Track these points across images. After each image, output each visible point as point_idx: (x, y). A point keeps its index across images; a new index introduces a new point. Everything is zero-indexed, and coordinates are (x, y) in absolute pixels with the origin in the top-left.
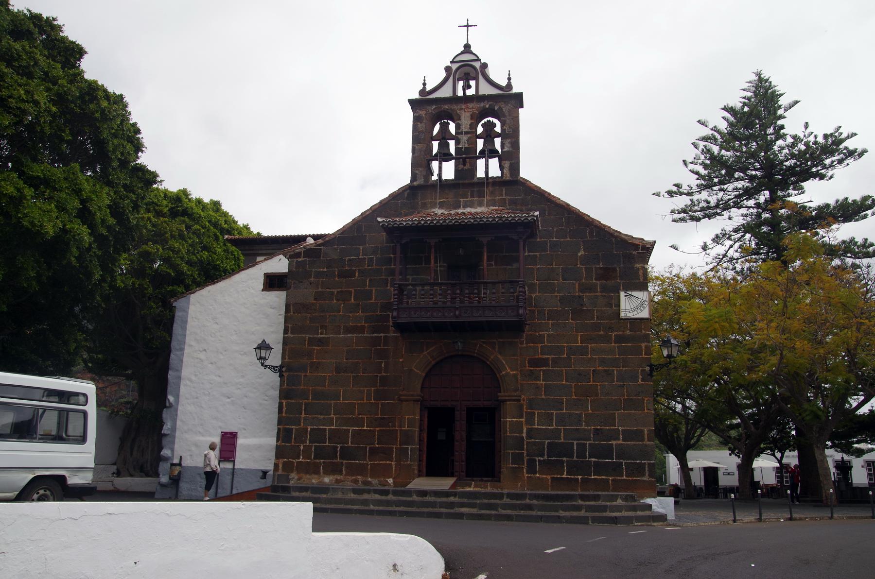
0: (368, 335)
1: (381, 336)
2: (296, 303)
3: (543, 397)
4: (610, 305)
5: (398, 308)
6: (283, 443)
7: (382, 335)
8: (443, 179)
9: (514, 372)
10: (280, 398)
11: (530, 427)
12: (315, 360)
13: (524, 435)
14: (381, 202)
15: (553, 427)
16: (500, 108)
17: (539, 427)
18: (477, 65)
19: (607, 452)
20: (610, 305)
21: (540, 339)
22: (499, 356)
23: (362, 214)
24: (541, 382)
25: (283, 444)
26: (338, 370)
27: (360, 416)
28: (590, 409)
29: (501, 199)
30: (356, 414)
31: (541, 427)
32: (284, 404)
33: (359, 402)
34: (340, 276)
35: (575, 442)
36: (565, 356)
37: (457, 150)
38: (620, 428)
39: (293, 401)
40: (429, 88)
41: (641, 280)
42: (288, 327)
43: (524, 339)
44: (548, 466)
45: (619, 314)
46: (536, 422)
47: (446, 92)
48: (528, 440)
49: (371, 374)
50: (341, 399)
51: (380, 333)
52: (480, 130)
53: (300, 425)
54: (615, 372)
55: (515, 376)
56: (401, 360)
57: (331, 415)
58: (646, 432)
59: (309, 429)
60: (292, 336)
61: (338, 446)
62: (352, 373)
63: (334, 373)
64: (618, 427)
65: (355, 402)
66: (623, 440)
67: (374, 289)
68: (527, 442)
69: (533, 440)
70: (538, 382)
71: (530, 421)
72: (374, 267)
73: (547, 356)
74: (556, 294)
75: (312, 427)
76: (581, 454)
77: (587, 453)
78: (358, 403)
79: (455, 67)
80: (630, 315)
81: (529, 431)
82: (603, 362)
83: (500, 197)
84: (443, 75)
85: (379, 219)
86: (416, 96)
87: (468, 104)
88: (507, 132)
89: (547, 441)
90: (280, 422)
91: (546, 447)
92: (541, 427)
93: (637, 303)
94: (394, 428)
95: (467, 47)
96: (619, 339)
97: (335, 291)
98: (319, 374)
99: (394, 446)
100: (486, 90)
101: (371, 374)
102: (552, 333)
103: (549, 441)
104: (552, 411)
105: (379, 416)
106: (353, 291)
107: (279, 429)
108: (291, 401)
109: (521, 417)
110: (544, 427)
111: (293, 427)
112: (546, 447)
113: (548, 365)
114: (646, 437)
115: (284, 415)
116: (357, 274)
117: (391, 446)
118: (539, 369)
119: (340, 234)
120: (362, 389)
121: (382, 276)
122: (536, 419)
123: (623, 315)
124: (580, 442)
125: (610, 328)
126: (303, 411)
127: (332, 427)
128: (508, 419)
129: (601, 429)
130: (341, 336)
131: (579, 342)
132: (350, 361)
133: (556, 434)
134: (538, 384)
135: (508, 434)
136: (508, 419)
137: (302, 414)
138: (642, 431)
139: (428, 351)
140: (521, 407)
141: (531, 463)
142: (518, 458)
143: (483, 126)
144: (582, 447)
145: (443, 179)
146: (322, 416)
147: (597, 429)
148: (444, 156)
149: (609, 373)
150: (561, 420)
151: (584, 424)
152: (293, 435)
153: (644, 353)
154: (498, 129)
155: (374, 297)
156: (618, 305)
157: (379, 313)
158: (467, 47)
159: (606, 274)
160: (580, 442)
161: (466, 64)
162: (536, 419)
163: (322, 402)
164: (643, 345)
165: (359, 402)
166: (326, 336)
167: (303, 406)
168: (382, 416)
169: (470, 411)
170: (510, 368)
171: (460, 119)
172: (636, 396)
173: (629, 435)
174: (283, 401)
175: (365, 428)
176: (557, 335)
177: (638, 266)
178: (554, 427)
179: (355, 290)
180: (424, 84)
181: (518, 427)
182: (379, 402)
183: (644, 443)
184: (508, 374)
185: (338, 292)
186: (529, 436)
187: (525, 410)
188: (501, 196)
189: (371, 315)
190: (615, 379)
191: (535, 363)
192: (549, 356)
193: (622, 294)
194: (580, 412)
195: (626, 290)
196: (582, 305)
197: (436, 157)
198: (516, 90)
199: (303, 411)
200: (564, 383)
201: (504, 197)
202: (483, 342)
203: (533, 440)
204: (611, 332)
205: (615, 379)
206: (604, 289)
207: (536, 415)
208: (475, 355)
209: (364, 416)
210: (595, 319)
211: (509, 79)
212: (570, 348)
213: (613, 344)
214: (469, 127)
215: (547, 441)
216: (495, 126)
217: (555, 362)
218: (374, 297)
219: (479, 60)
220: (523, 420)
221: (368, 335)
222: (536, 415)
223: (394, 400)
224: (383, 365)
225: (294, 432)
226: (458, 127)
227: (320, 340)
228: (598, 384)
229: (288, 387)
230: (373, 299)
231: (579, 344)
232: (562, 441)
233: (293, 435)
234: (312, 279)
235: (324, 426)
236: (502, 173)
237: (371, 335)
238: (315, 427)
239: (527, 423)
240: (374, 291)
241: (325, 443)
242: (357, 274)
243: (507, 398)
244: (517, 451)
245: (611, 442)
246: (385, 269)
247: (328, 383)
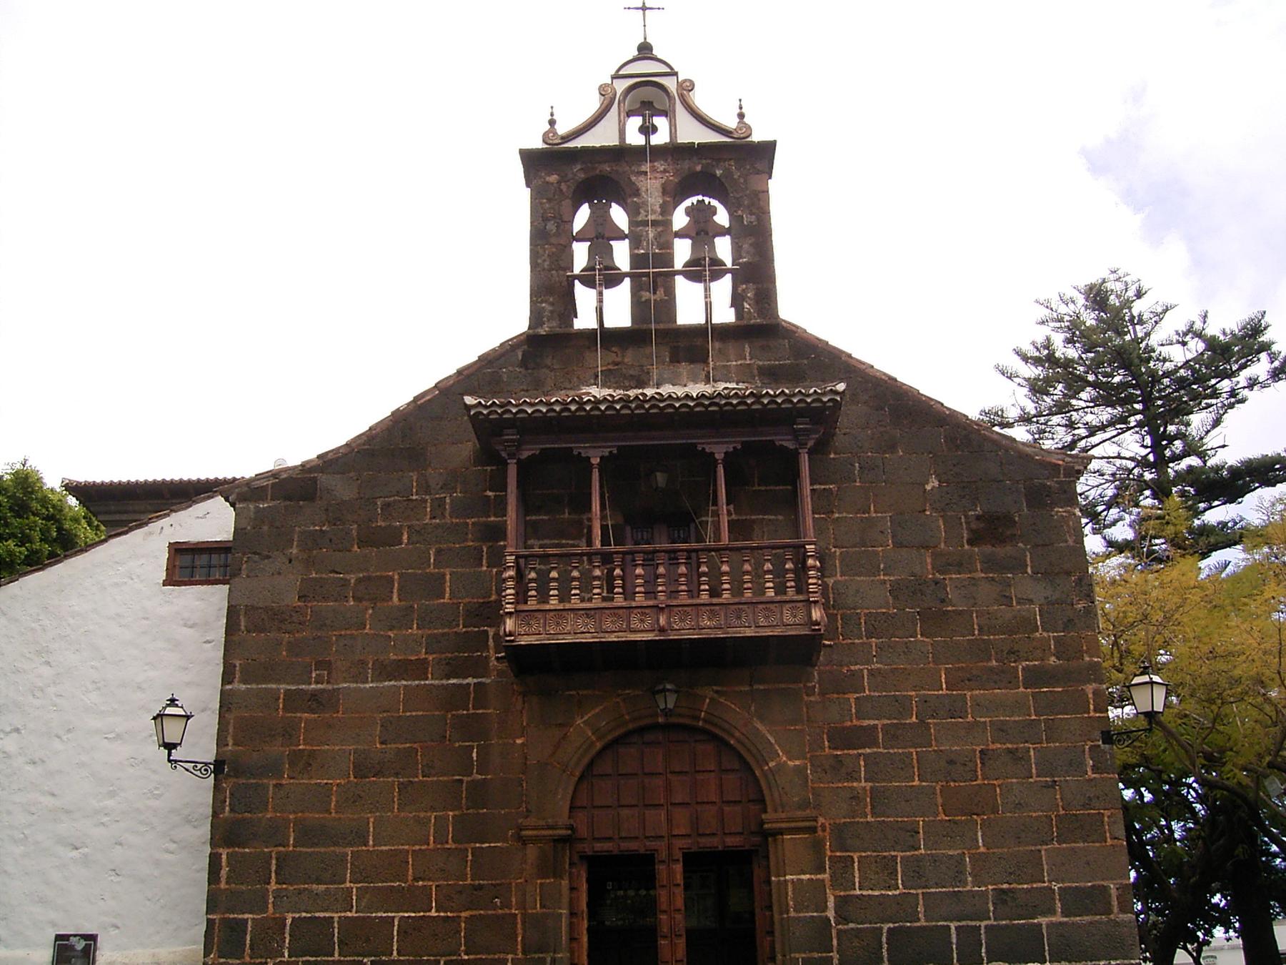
0: (436, 682)
1: (469, 684)
2: (254, 608)
3: (869, 819)
5: (516, 611)
6: (219, 957)
7: (470, 680)
8: (688, 218)
9: (797, 763)
10: (213, 843)
11: (842, 894)
12: (301, 747)
13: (831, 914)
14: (459, 372)
15: (897, 892)
16: (728, 174)
17: (865, 893)
18: (670, 83)
21: (854, 682)
22: (759, 726)
23: (416, 399)
24: (863, 784)
25: (222, 960)
26: (361, 770)
27: (421, 883)
28: (981, 844)
29: (741, 364)
30: (410, 878)
31: (870, 892)
32: (224, 857)
33: (417, 847)
34: (362, 543)
35: (953, 925)
36: (914, 719)
37: (636, 260)
38: (1056, 887)
39: (247, 850)
40: (562, 129)
41: (1071, 542)
42: (235, 666)
43: (815, 682)
46: (857, 880)
47: (602, 137)
48: (840, 927)
49: (445, 778)
50: (371, 843)
51: (466, 678)
52: (680, 219)
53: (265, 909)
54: (1032, 753)
55: (800, 771)
56: (519, 741)
57: (344, 882)
58: (1114, 893)
59: (289, 921)
60: (243, 687)
61: (365, 960)
62: (397, 775)
63: (352, 778)
64: (1050, 881)
65: (406, 847)
66: (1064, 914)
67: (447, 571)
68: (839, 932)
69: (852, 925)
70: (855, 784)
72: (448, 520)
73: (872, 722)
74: (882, 577)
75: (297, 915)
77: (983, 950)
78: (414, 851)
79: (621, 86)
81: (842, 903)
82: (1001, 730)
83: (739, 363)
84: (594, 105)
85: (469, 400)
86: (537, 143)
87: (656, 164)
88: (745, 223)
89: (886, 927)
90: (212, 905)
91: (884, 939)
92: (870, 892)
94: (507, 911)
95: (645, 51)
96: (1035, 678)
97: (353, 578)
98: (313, 782)
99: (510, 957)
100: (692, 133)
101: (445, 778)
102: (879, 666)
103: (891, 925)
104: (893, 853)
105: (469, 882)
106: (396, 577)
107: (210, 923)
108: (241, 850)
109: (821, 869)
110: (876, 893)
111: (246, 916)
112: (884, 939)
113: (874, 743)
114: (1115, 903)
115: (223, 885)
116: (405, 537)
117: (502, 956)
118: (855, 752)
119: (364, 444)
120: (422, 815)
121: (466, 540)
122: (857, 875)
124: (964, 923)
125: (1011, 652)
126: (273, 875)
127: (349, 914)
128: (788, 877)
129: (1009, 890)
130: (367, 686)
131: (944, 686)
132: (393, 746)
133: (904, 907)
134: (852, 788)
135: (792, 914)
136: (788, 877)
137: (269, 883)
139: (586, 718)
140: (818, 846)
143: (689, 211)
144: (968, 935)
145: (688, 218)
146: (322, 887)
147: (1002, 890)
148: (602, 276)
149: (1017, 757)
150: (916, 873)
151: (970, 879)
152: (248, 938)
153: (1092, 707)
154: (722, 217)
155: (448, 589)
157: (461, 629)
158: (645, 51)
160: (964, 923)
161: (647, 82)
162: (857, 875)
163: (323, 850)
164: (1090, 689)
165: (417, 847)
166: (330, 687)
167: (274, 862)
168: (477, 882)
169: (693, 861)
170: (786, 753)
171: (637, 193)
172: (1084, 806)
173: (1080, 901)
174: (221, 850)
175: (433, 913)
176: (893, 671)
178: (901, 889)
179: (401, 575)
180: (552, 123)
181: (815, 895)
182: (466, 845)
183: (1112, 917)
185: (359, 581)
186: (842, 917)
187: (829, 853)
188: (741, 359)
189: (443, 635)
190: (1034, 771)
191: (847, 738)
192: (876, 722)
194: (960, 851)
196: (943, 601)
197: (588, 281)
198: (756, 137)
199: (273, 875)
200: (916, 783)
201: (748, 362)
202: (717, 692)
203: (852, 925)
204: (1015, 662)
205: (1034, 771)
207: (856, 864)
208: (701, 724)
209: (431, 883)
210: (976, 632)
211: (741, 116)
213: (1022, 689)
214: (659, 210)
215: (886, 927)
216: (713, 211)
217: (893, 735)
218: (448, 589)
219: (674, 74)
220: (826, 876)
221: (436, 682)
222: (856, 864)
223: (505, 840)
224: (474, 755)
225: (250, 929)
226: (632, 211)
227: (314, 696)
228: (995, 782)
229: (232, 815)
230: (447, 595)
231: (944, 692)
232: (923, 923)
233: (248, 938)
234: (295, 551)
235: (326, 911)
236: (739, 314)
237: (444, 682)
238: (304, 914)
239: (836, 882)
240: (448, 577)
241: (332, 955)
242: (405, 537)
243: (784, 825)
244: (816, 955)
245: (1036, 921)
246: (473, 524)
247: (337, 801)
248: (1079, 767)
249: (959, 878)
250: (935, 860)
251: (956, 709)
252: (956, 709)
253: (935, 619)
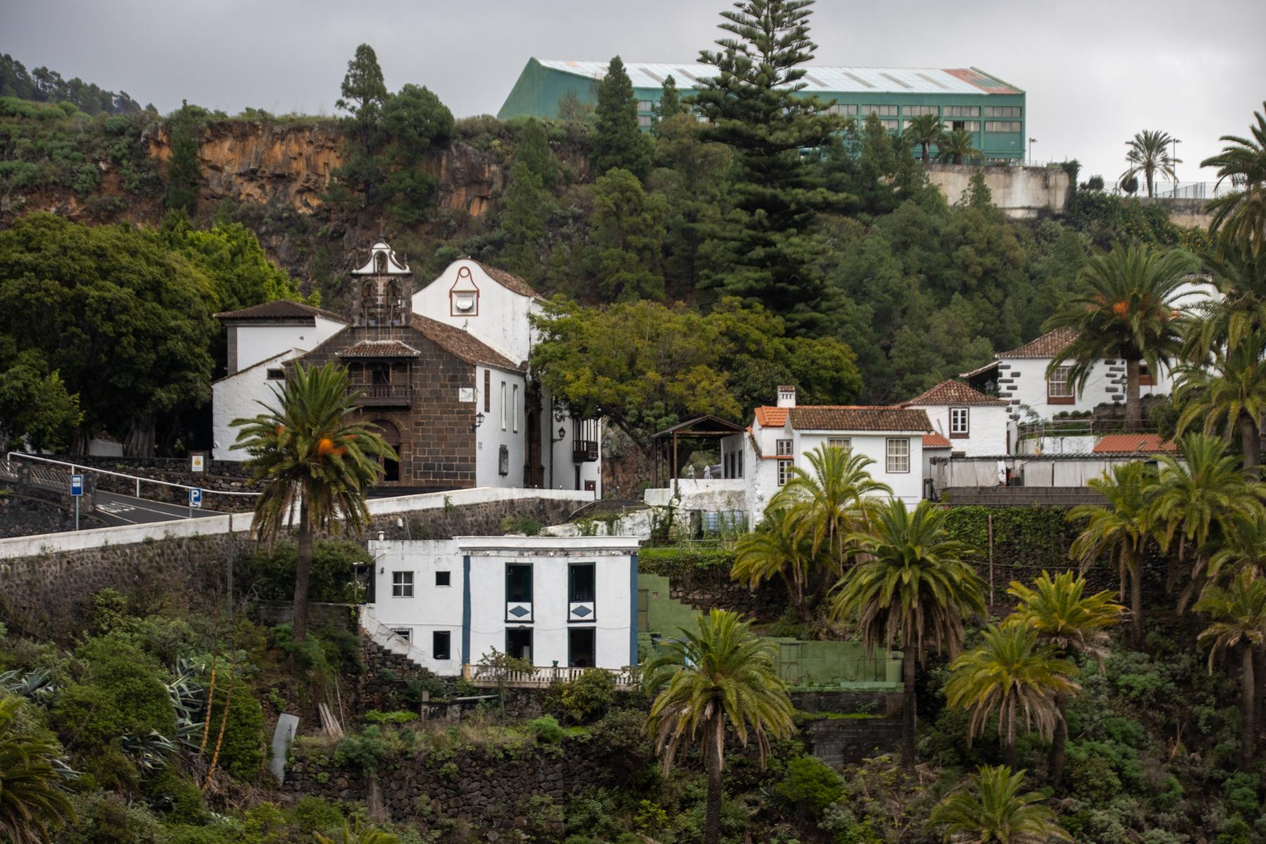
19: (451, 467)
21: (419, 412)
44: (424, 475)
133: (427, 459)
142: (409, 471)
150: (430, 452)
159: (453, 379)
173: (462, 459)
181: (409, 456)
191: (418, 424)
206: (452, 386)
251: (441, 418)
252: (441, 418)
253: (439, 399)
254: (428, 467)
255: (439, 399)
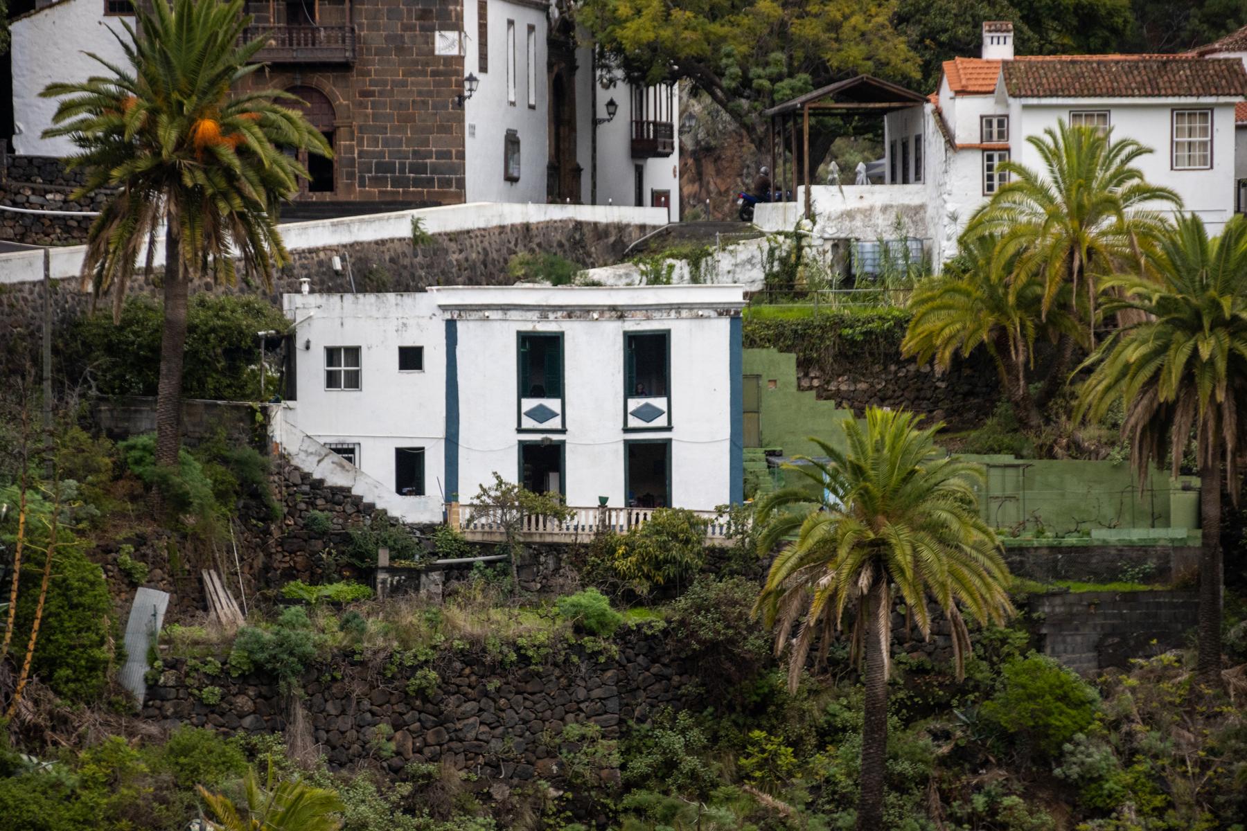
4: (427, 43)
19: (421, 169)
20: (427, 43)
21: (368, 73)
44: (376, 181)
45: (433, 50)
55: (348, 106)
71: (361, 141)
76: (402, 170)
80: (443, 53)
81: (361, 154)
82: (420, 93)
93: (448, 43)
96: (434, 74)
123: (437, 53)
133: (382, 154)
138: (450, 152)
140: (352, 133)
141: (362, 179)
142: (351, 176)
144: (403, 166)
149: (425, 103)
156: (433, 43)
159: (424, 15)
164: (454, 79)
173: (440, 155)
177: (452, 7)
184: (341, 104)
186: (360, 156)
191: (365, 94)
193: (437, 34)
195: (440, 30)
206: (423, 28)
212: (393, 81)
217: (381, 93)
248: (447, 107)
249: (400, 145)
250: (393, 139)
251: (403, 84)
253: (400, 50)
254: (383, 168)
255: (400, 50)
